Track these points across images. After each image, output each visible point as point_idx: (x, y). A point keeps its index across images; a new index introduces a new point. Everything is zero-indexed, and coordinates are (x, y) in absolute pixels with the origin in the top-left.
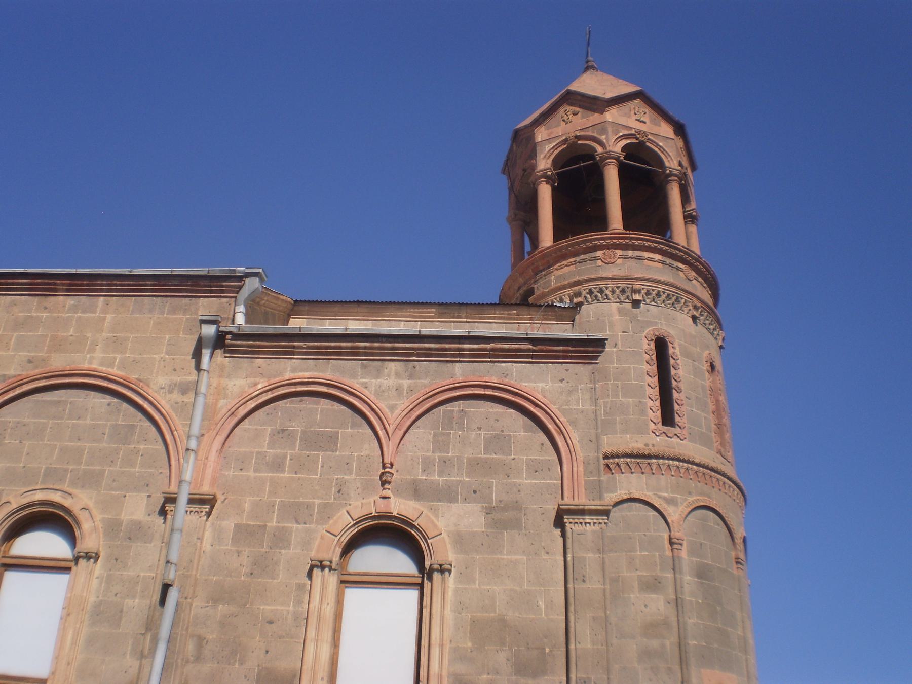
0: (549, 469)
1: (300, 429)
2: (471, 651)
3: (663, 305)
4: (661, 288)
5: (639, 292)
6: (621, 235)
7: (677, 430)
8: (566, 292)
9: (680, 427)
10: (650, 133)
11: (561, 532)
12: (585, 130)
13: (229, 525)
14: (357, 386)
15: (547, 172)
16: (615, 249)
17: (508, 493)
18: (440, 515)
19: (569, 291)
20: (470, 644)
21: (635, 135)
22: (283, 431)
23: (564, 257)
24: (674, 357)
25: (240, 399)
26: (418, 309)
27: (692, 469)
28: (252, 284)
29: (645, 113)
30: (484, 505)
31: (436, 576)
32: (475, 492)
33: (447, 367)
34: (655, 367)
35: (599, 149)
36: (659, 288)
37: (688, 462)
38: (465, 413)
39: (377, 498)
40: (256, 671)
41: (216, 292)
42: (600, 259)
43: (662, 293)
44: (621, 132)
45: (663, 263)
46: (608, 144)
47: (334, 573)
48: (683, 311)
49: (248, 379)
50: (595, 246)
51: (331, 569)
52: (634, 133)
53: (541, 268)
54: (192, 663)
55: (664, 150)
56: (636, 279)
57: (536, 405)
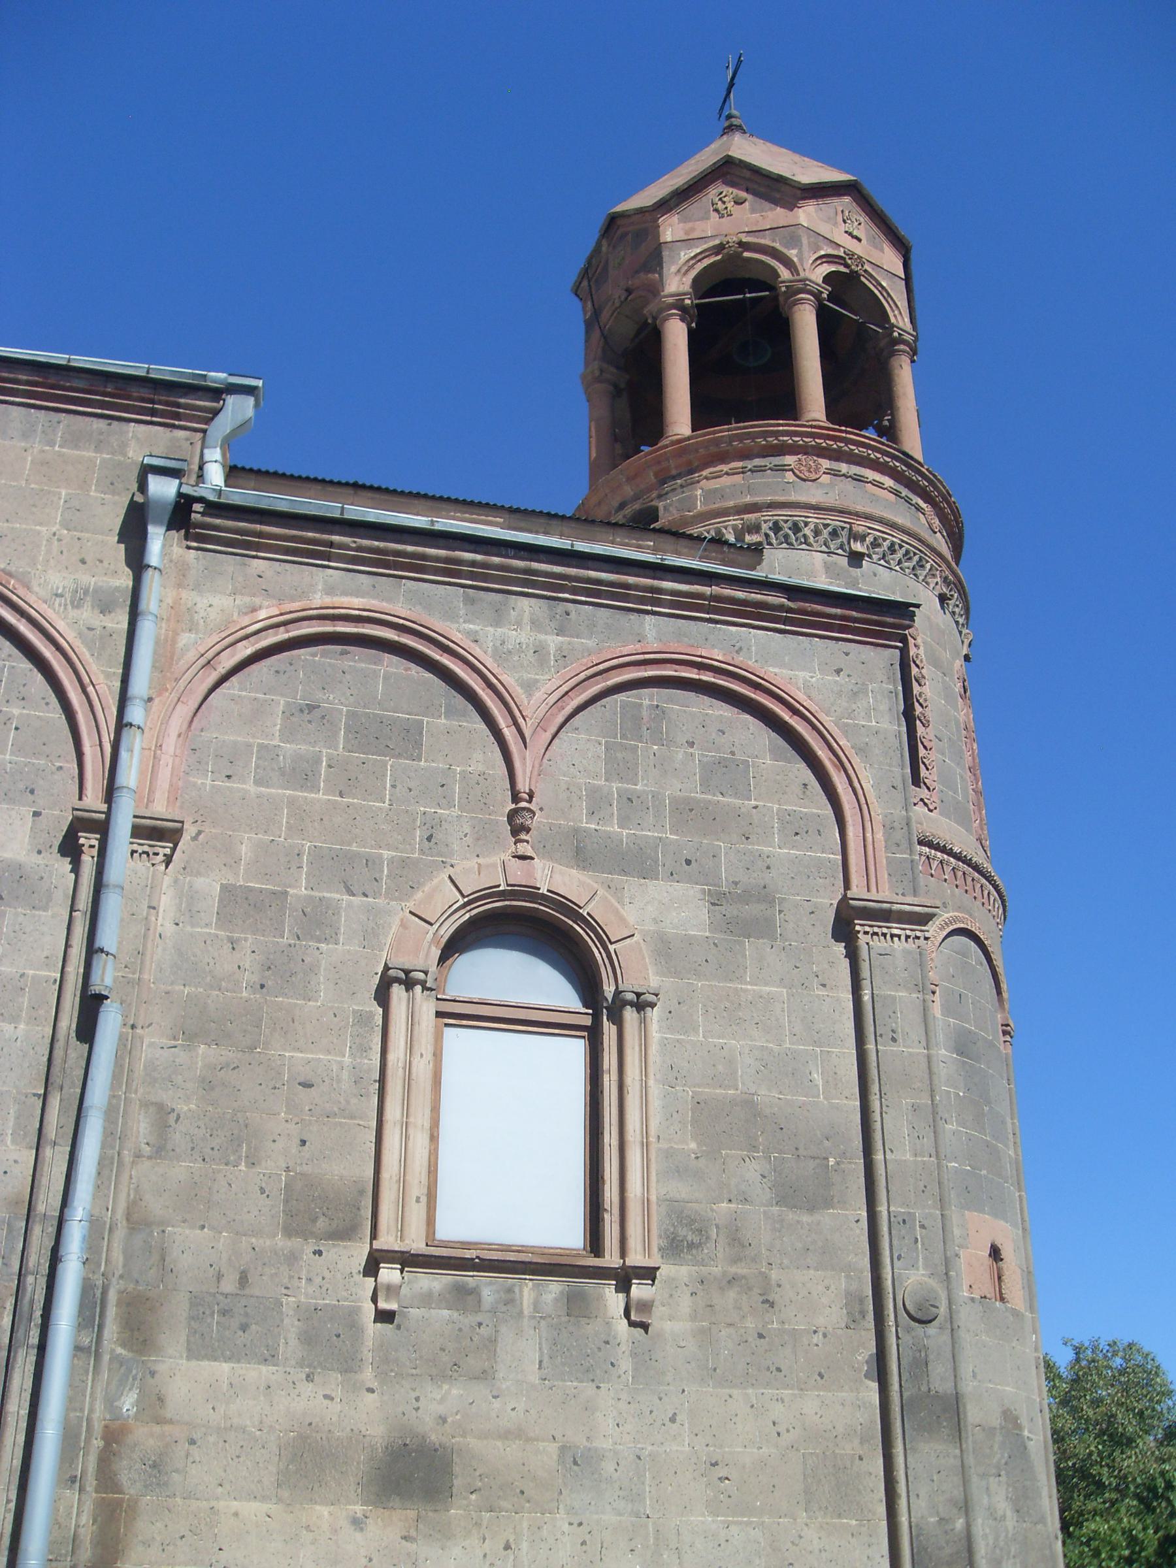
0: (819, 831)
1: (345, 709)
2: (697, 1158)
3: (897, 568)
4: (897, 537)
5: (862, 538)
6: (831, 433)
8: (729, 521)
9: (928, 788)
10: (868, 261)
11: (845, 947)
12: (757, 233)
13: (210, 885)
14: (457, 636)
15: (684, 299)
16: (818, 456)
17: (748, 869)
18: (627, 900)
19: (734, 521)
20: (693, 1145)
21: (843, 259)
22: (311, 708)
23: (723, 458)
24: (917, 662)
25: (223, 635)
26: (472, 514)
27: (948, 863)
29: (860, 224)
30: (706, 887)
31: (629, 1014)
32: (688, 862)
33: (630, 619)
35: (785, 274)
36: (893, 536)
38: (663, 712)
39: (506, 856)
40: (283, 1179)
41: (162, 414)
42: (792, 470)
43: (897, 547)
44: (822, 249)
45: (897, 493)
46: (802, 265)
47: (429, 996)
48: (927, 583)
49: (238, 597)
50: (782, 445)
52: (843, 255)
53: (674, 472)
54: (150, 1158)
56: (858, 515)
57: (795, 712)
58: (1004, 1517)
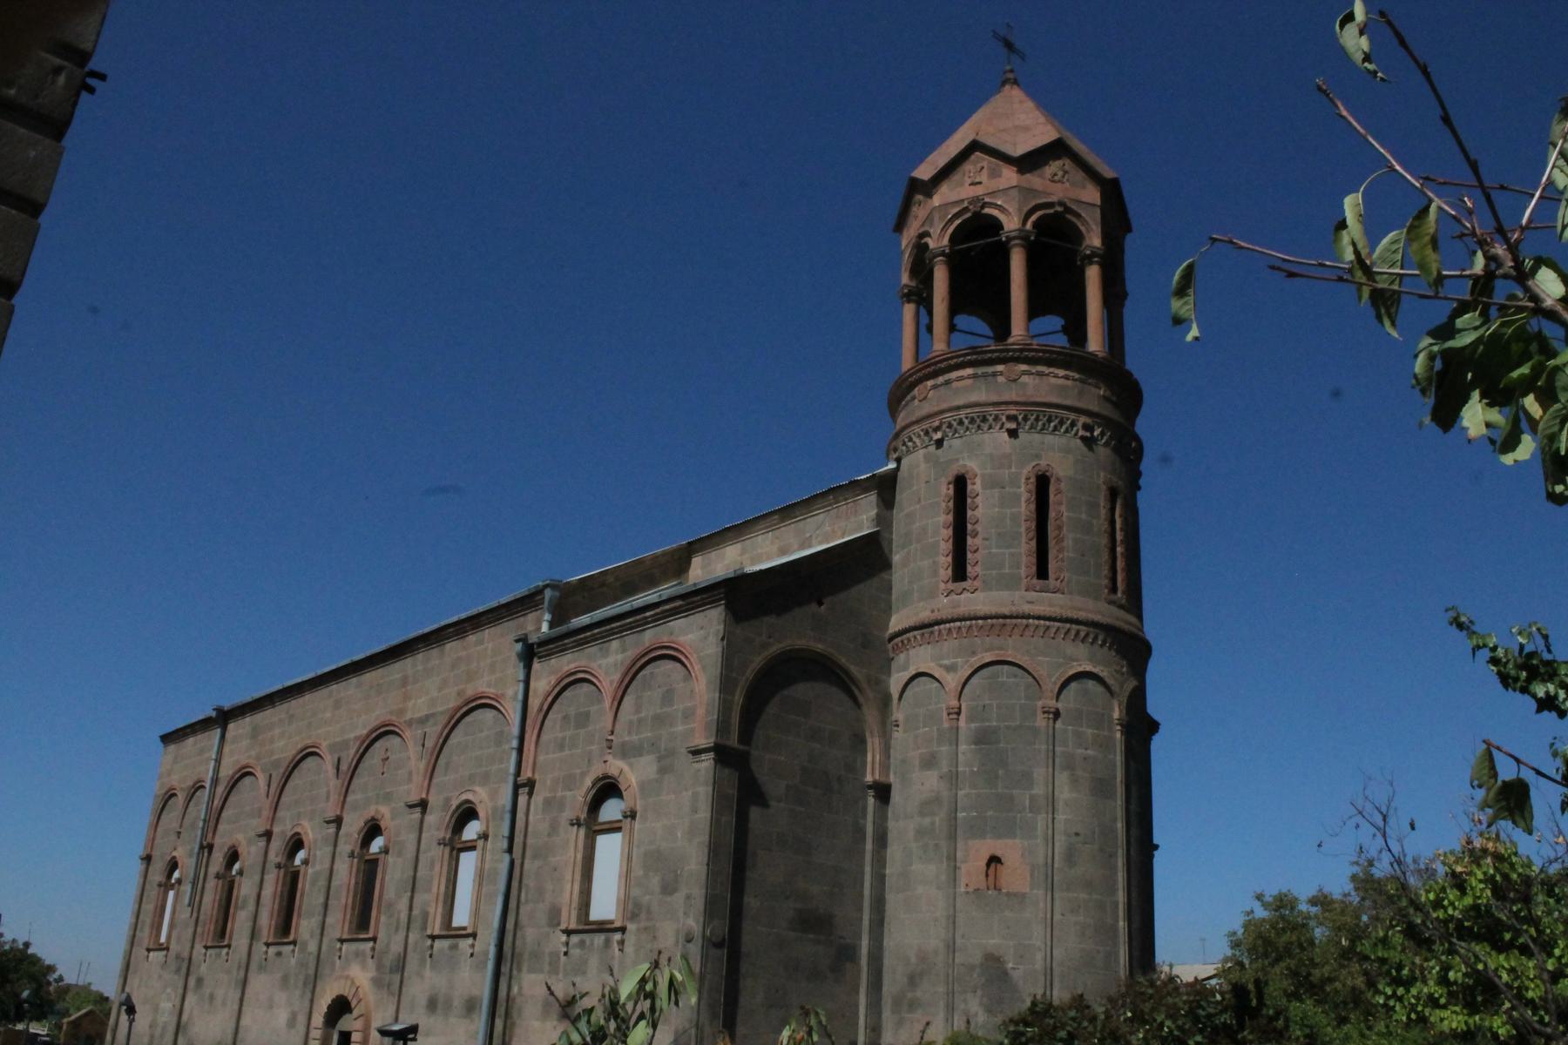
3: (968, 433)
5: (936, 429)
7: (969, 581)
27: (977, 625)
28: (548, 593)
32: (653, 744)
34: (950, 518)
37: (971, 619)
45: (975, 376)
51: (579, 825)
55: (1004, 209)
58: (976, 1015)
